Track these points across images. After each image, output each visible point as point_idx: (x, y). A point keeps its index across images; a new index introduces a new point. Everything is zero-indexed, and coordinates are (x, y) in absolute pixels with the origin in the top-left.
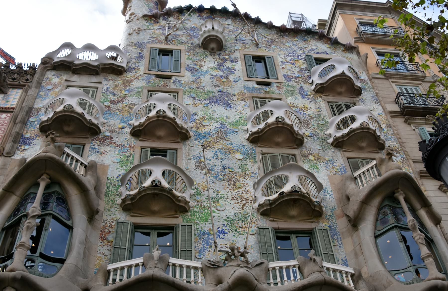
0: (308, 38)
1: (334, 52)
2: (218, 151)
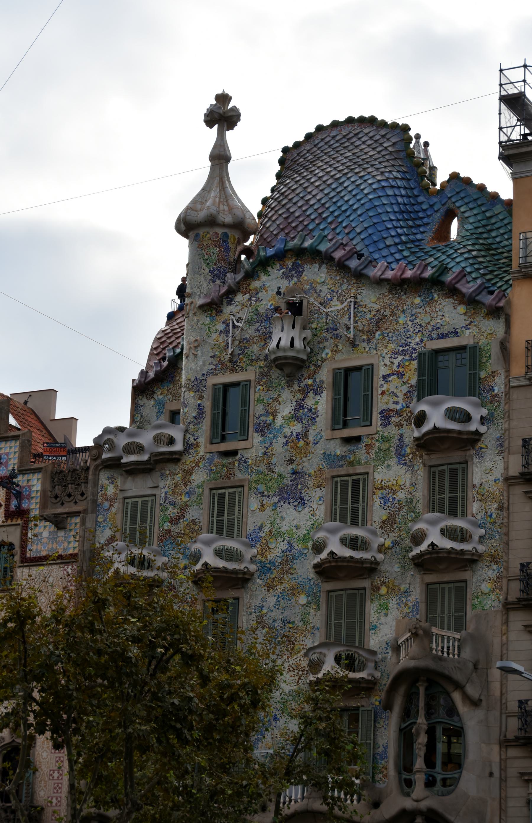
0: (435, 291)
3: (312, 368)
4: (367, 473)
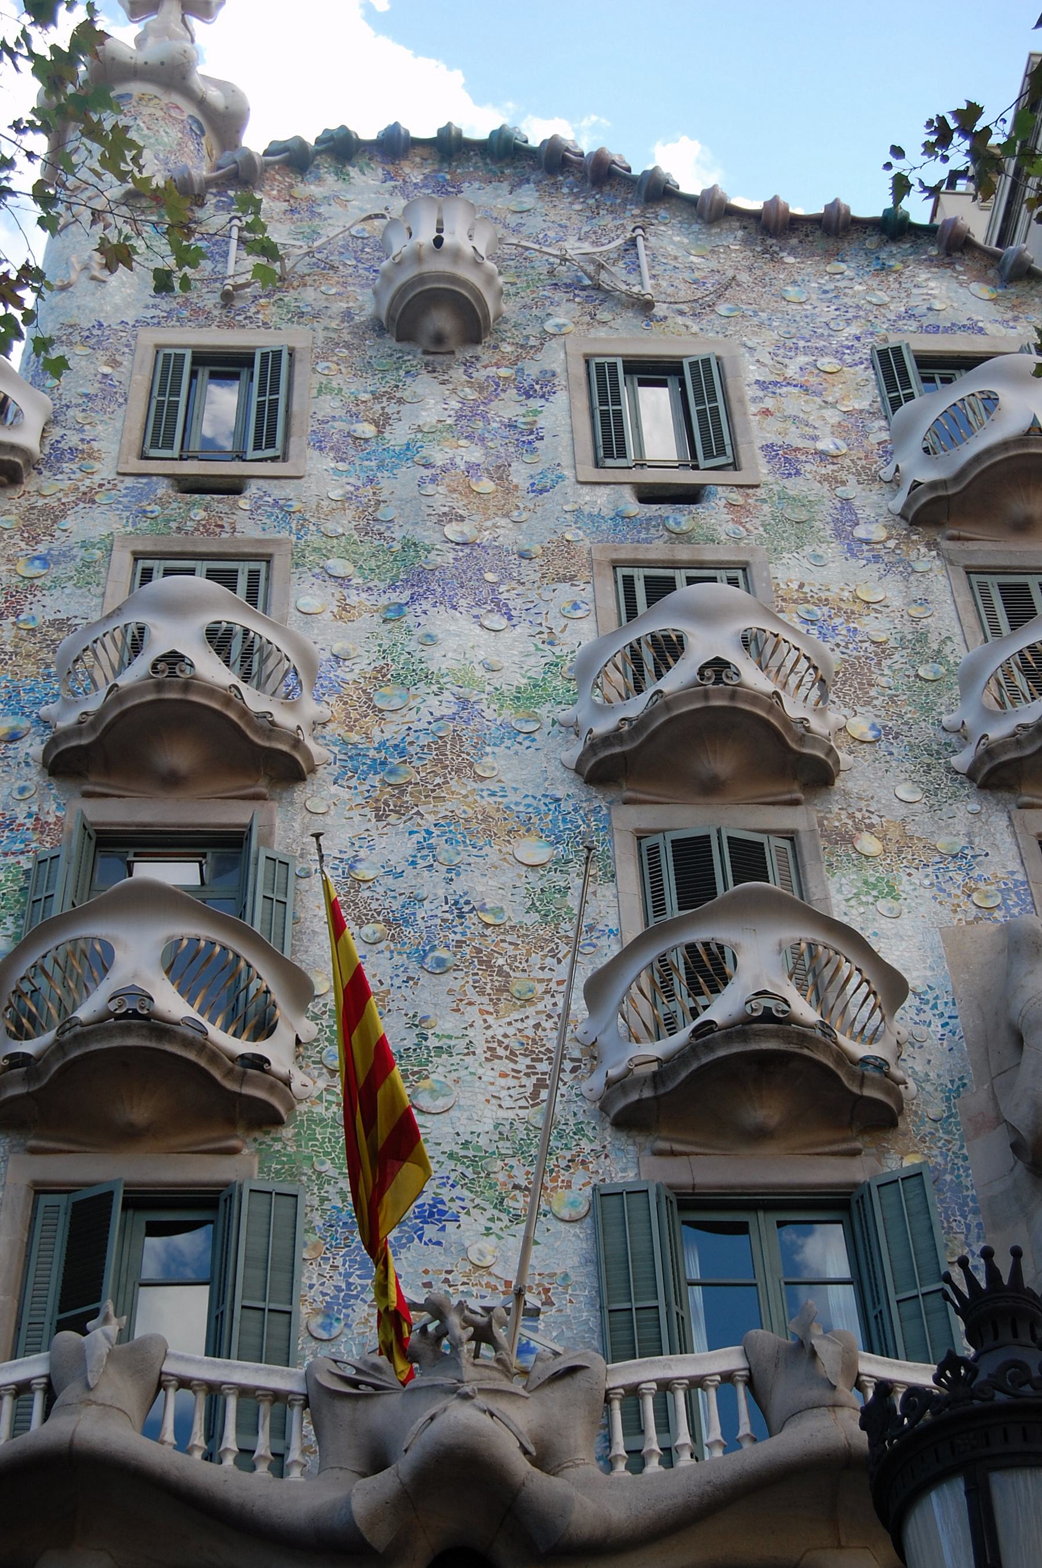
0: (892, 255)
1: (1016, 319)
2: (436, 832)
3: (507, 348)
4: (744, 567)
